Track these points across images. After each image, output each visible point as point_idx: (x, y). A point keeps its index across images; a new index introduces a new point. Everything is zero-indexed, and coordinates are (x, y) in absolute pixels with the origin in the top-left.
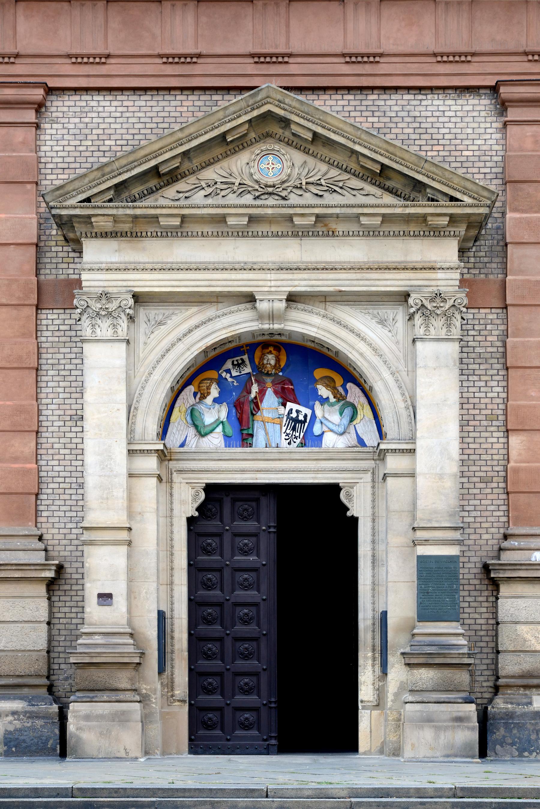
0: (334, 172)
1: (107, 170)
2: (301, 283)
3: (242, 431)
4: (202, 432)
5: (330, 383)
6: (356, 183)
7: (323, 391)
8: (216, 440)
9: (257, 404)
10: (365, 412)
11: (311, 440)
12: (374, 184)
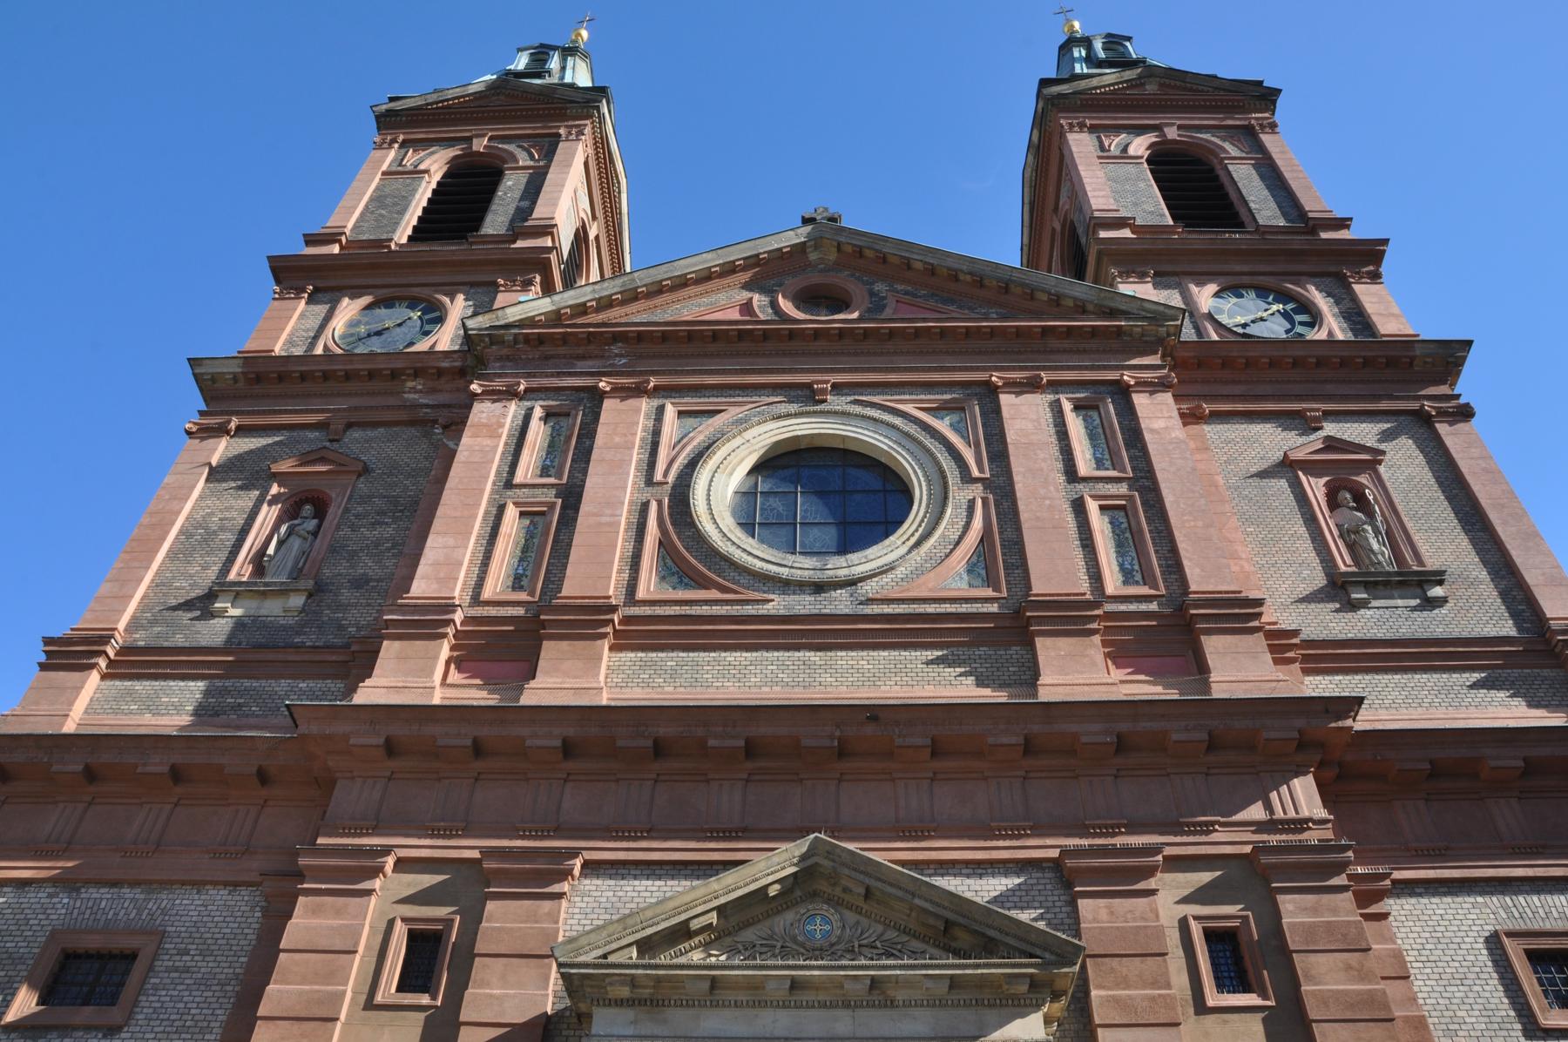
0: (891, 934)
1: (630, 921)
6: (916, 945)
12: (938, 946)
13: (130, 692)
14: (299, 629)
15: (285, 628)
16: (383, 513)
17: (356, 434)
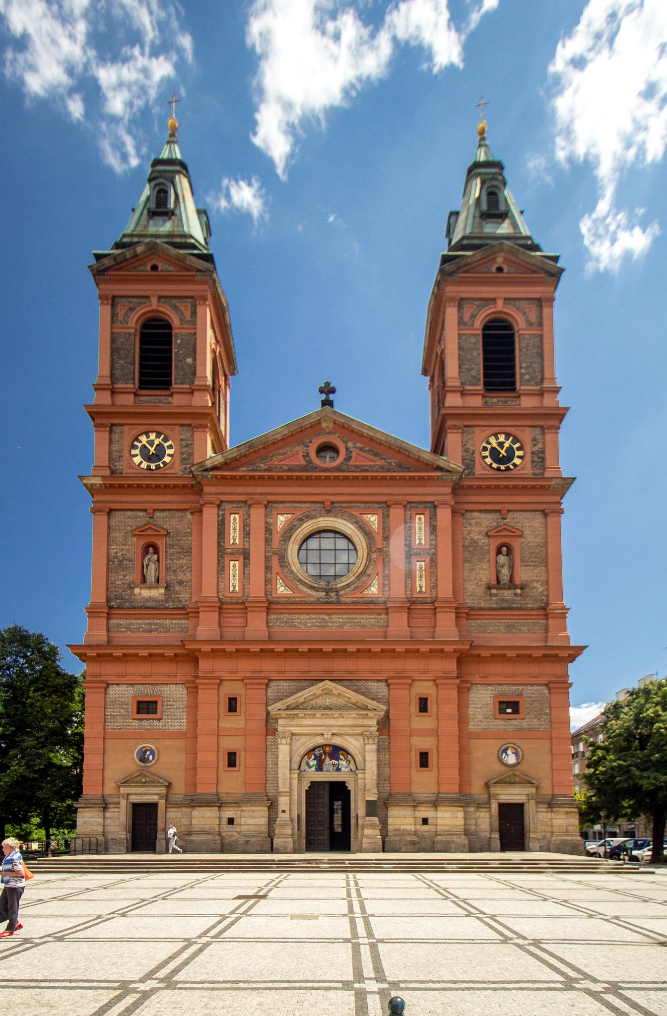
2: (335, 730)
3: (320, 768)
4: (310, 767)
5: (343, 755)
7: (341, 757)
8: (313, 769)
9: (324, 761)
10: (352, 762)
11: (338, 770)
13: (119, 625)
14: (166, 601)
15: (162, 601)
16: (179, 553)
17: (158, 514)
